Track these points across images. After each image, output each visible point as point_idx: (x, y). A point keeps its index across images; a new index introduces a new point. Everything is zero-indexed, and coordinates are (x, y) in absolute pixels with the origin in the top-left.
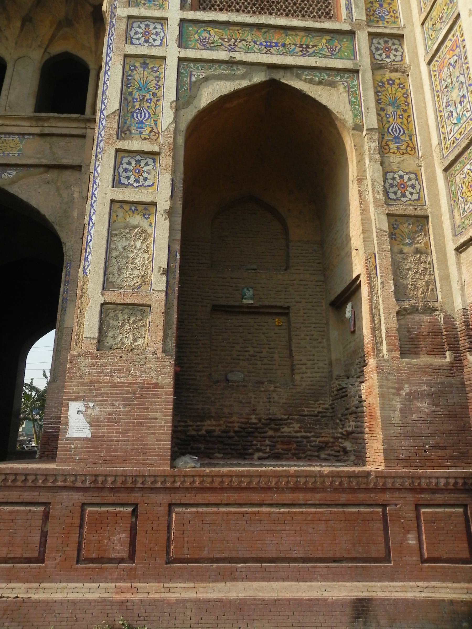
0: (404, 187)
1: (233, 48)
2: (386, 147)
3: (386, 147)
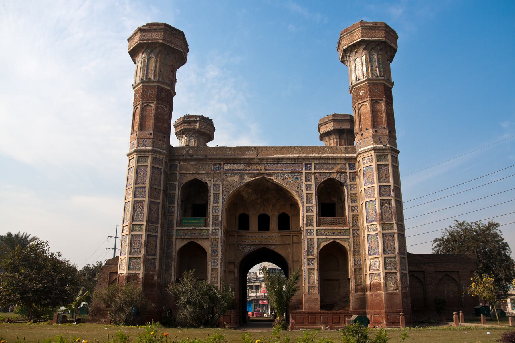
1: (326, 235)
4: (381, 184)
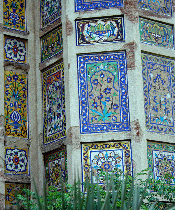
0: (17, 161)
2: (9, 130)
3: (9, 130)
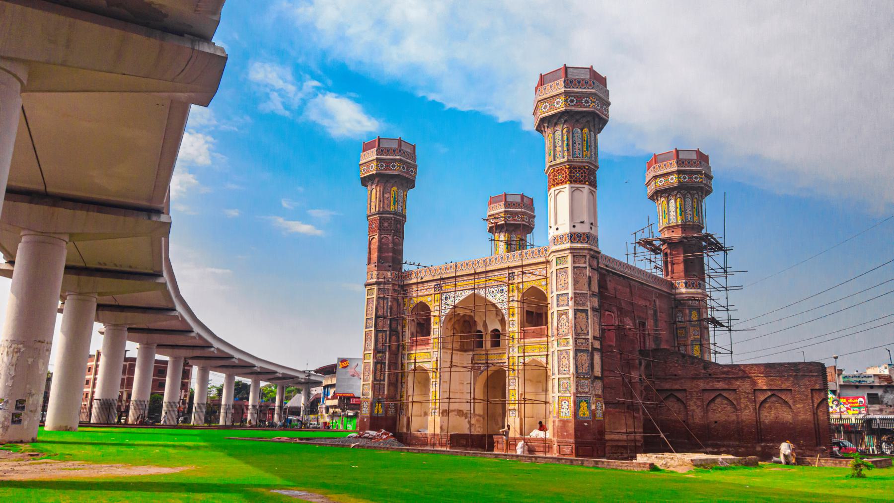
4: (559, 293)
